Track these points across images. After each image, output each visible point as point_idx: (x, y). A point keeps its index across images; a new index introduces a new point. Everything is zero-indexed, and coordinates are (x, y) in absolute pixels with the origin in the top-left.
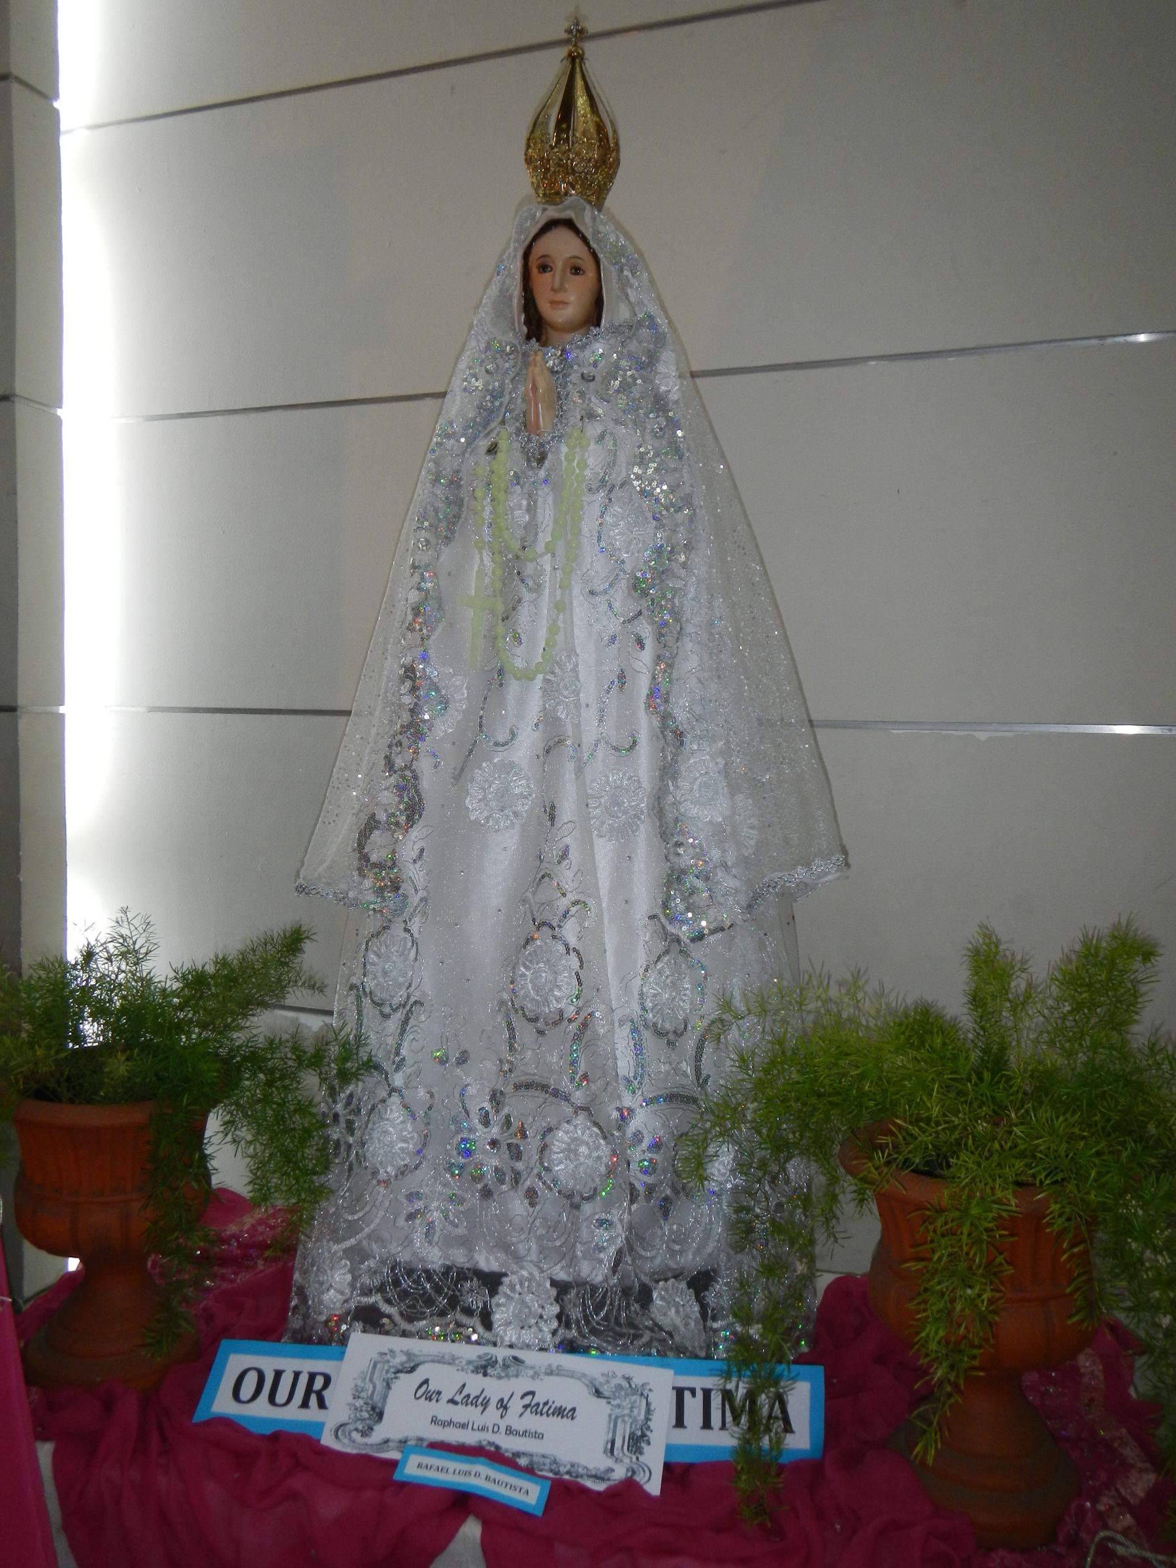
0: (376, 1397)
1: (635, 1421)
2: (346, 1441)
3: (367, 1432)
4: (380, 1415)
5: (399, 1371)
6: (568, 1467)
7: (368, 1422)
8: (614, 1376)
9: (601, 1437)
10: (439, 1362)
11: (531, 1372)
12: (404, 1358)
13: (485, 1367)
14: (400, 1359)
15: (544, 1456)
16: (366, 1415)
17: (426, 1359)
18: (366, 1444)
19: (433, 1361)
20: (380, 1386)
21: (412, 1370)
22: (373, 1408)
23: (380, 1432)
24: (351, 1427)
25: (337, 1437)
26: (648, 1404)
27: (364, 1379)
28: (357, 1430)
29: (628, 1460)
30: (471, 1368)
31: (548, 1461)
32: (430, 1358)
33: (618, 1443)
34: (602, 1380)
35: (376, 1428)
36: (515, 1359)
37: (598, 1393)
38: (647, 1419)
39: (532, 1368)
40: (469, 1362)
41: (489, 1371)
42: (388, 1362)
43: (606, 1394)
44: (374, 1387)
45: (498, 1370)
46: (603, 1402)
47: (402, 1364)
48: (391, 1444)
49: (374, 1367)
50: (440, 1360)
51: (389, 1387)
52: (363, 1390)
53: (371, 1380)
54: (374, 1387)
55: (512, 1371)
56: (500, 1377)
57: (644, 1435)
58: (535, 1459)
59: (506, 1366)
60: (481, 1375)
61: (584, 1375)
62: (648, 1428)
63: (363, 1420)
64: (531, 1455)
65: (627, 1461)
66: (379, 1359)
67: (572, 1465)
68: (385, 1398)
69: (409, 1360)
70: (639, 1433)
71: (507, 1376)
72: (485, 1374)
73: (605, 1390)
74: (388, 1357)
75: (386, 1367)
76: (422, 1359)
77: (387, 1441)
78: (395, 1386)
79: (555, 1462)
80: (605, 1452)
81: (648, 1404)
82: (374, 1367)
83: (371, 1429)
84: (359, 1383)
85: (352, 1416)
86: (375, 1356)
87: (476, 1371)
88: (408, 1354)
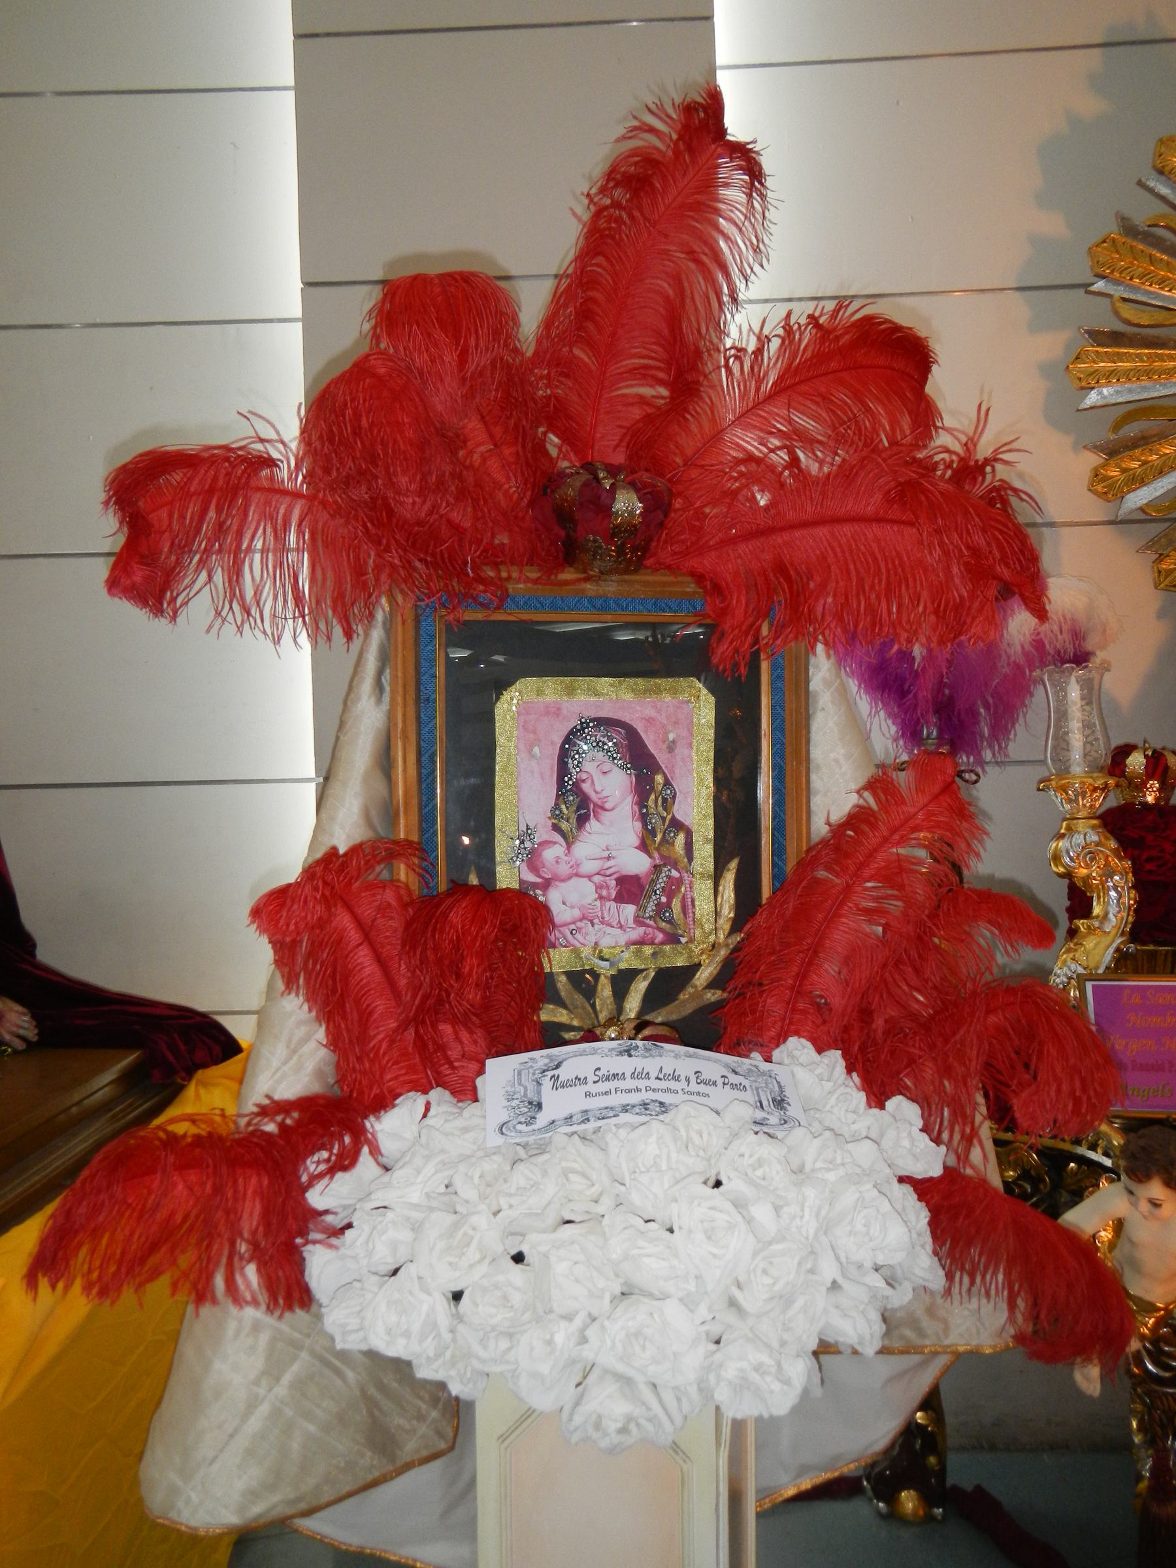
0: (530, 1095)
2: (513, 1134)
4: (539, 1106)
5: (544, 1071)
7: (529, 1114)
10: (581, 1055)
12: (546, 1061)
16: (526, 1110)
17: (568, 1056)
18: (534, 1130)
19: (575, 1056)
20: (531, 1086)
21: (557, 1066)
22: (530, 1103)
24: (515, 1122)
25: (502, 1134)
28: (520, 1123)
30: (614, 1053)
32: (571, 1055)
35: (537, 1116)
41: (633, 1053)
42: (532, 1067)
44: (526, 1088)
47: (546, 1065)
48: (557, 1123)
49: (519, 1074)
51: (539, 1084)
52: (514, 1094)
53: (520, 1084)
54: (526, 1088)
60: (626, 1057)
66: (522, 1067)
68: (539, 1093)
69: (552, 1060)
72: (630, 1056)
74: (530, 1064)
75: (531, 1071)
76: (564, 1057)
82: (519, 1074)
83: (534, 1118)
84: (509, 1089)
85: (512, 1114)
87: (621, 1054)
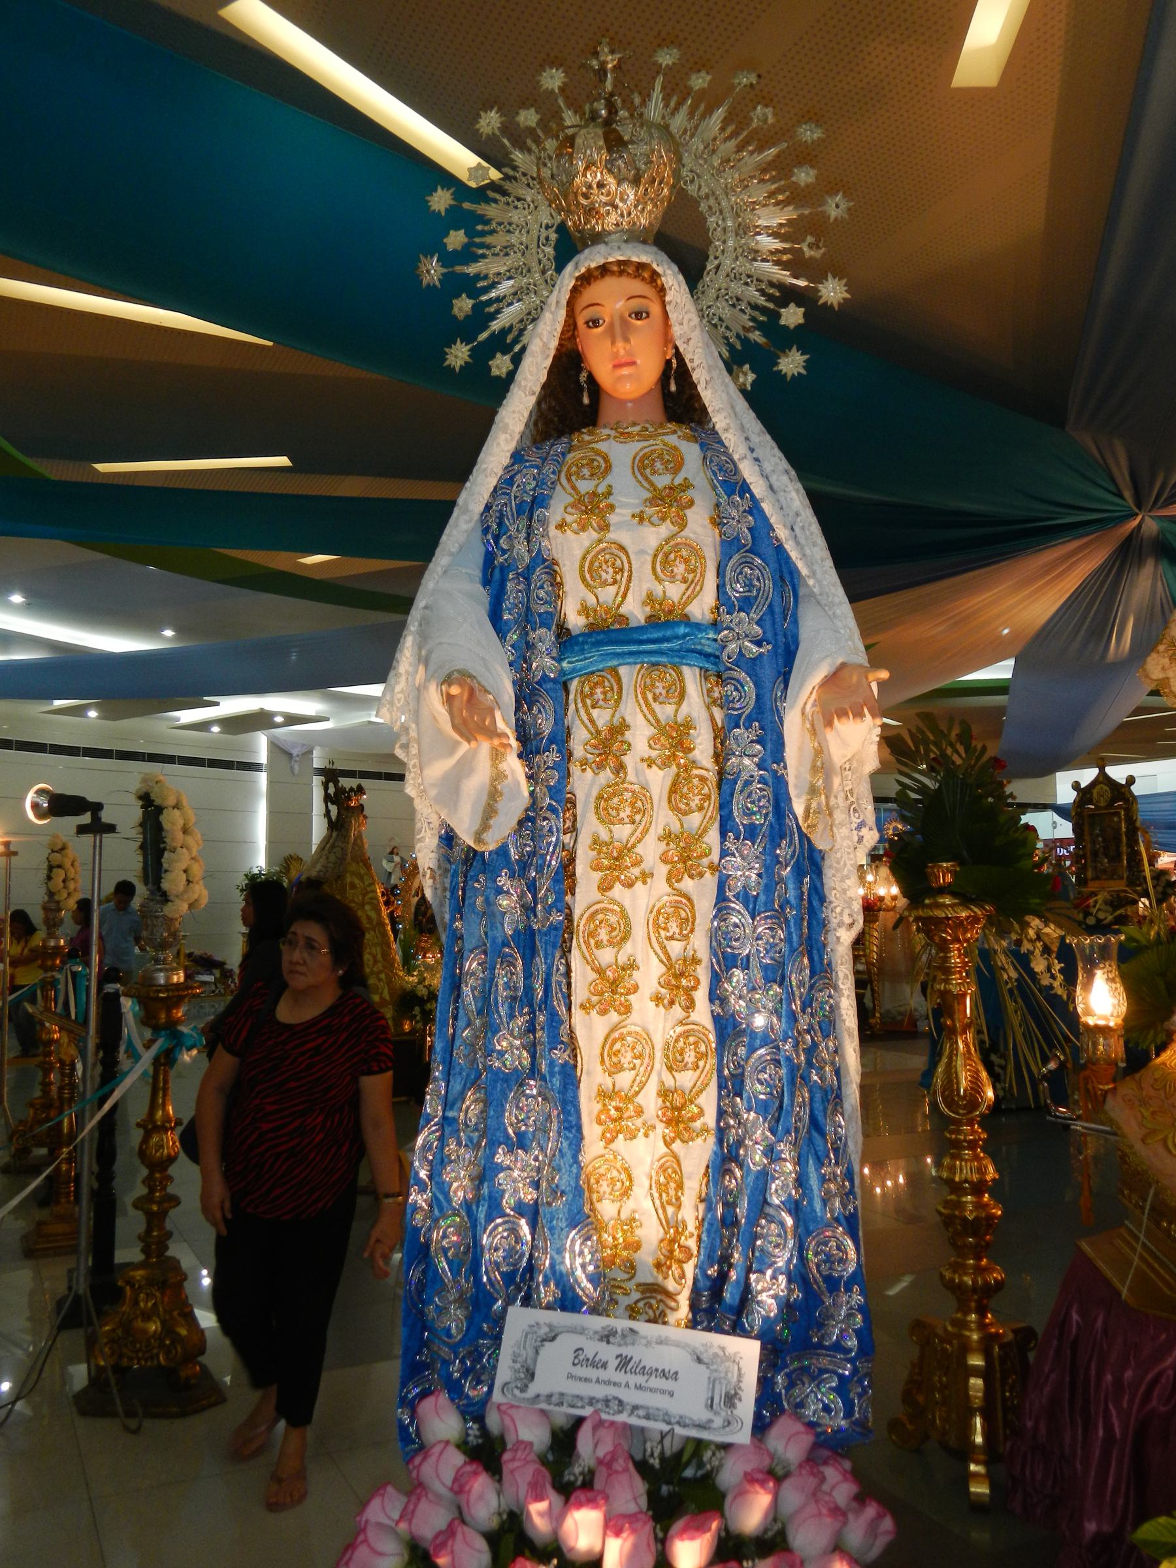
1: (729, 1382)
3: (524, 1389)
4: (532, 1376)
5: (543, 1340)
6: (677, 1419)
8: (712, 1346)
9: (703, 1396)
11: (644, 1342)
12: (546, 1329)
13: (607, 1337)
14: (544, 1330)
15: (658, 1409)
16: (522, 1376)
20: (531, 1352)
21: (553, 1339)
22: (527, 1370)
23: (534, 1389)
24: (513, 1385)
26: (739, 1369)
27: (519, 1348)
29: (725, 1413)
30: (597, 1337)
31: (661, 1413)
33: (716, 1400)
34: (702, 1349)
36: (631, 1330)
37: (699, 1360)
38: (739, 1381)
39: (645, 1338)
40: (596, 1332)
41: (611, 1339)
43: (706, 1360)
45: (618, 1339)
46: (703, 1367)
49: (526, 1337)
50: (573, 1330)
51: (537, 1353)
55: (629, 1340)
56: (620, 1345)
57: (736, 1394)
58: (651, 1411)
59: (624, 1336)
61: (687, 1345)
62: (740, 1388)
63: (521, 1379)
64: (647, 1408)
65: (723, 1414)
67: (681, 1417)
68: (535, 1361)
69: (551, 1330)
70: (733, 1392)
71: (626, 1344)
72: (608, 1342)
73: (704, 1357)
77: (538, 1396)
78: (542, 1352)
79: (667, 1414)
80: (706, 1405)
81: (739, 1369)
83: (526, 1386)
86: (527, 1329)
87: (601, 1339)
88: (550, 1326)
